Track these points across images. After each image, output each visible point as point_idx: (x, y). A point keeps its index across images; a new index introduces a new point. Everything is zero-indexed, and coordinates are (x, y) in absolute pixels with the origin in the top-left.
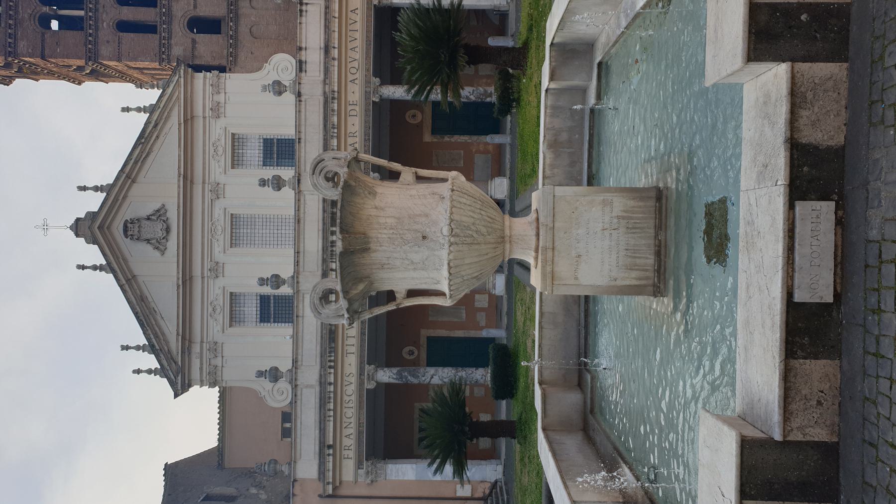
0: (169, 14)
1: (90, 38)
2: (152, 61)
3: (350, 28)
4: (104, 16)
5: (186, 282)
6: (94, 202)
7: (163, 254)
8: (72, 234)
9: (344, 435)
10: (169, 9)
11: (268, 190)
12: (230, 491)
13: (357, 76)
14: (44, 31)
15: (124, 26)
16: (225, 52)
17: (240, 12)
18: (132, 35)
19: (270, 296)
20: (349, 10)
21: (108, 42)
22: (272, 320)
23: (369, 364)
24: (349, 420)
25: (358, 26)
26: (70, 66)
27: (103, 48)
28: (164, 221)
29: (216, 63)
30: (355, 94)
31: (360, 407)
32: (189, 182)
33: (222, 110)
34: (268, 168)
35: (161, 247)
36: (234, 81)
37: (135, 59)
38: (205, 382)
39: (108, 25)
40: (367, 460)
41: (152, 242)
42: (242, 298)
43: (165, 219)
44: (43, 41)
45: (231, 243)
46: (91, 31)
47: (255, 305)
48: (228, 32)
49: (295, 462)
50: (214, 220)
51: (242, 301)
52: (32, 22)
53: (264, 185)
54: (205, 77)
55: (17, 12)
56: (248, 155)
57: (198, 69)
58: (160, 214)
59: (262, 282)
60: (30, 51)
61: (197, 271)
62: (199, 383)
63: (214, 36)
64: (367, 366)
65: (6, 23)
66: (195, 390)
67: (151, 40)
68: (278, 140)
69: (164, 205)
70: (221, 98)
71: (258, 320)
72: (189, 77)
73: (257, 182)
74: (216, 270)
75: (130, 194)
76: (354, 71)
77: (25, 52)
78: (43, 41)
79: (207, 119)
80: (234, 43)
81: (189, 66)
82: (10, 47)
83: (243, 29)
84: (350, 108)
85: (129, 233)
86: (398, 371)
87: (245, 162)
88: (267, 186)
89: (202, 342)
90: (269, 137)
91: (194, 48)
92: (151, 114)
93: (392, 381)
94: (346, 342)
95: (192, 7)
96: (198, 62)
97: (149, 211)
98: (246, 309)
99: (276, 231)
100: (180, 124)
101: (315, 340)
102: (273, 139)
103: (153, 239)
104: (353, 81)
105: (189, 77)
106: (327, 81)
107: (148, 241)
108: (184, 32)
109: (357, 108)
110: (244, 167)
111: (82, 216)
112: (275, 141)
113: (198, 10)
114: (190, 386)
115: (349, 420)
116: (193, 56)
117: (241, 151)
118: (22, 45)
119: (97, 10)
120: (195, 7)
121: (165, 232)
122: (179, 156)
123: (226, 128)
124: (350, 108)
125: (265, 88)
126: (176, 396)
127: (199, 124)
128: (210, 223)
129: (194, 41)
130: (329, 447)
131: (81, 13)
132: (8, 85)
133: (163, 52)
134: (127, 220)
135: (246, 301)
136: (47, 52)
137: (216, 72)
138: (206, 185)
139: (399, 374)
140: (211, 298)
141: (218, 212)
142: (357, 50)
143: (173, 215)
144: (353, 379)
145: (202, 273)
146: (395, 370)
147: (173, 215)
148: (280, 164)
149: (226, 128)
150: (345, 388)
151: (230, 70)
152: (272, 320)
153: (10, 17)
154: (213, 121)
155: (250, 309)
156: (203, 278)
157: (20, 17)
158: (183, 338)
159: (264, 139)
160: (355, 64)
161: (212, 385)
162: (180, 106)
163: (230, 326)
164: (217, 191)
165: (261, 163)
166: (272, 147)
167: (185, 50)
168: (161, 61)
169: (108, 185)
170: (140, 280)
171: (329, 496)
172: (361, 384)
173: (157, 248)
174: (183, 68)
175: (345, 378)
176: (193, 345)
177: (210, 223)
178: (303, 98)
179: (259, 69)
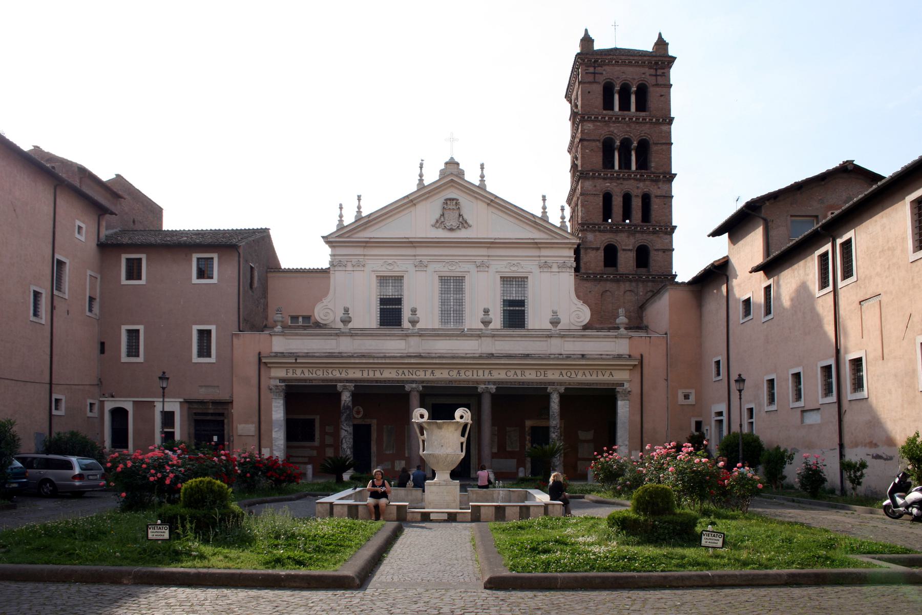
0: (617, 232)
1: (597, 174)
2: (582, 218)
3: (600, 372)
4: (615, 184)
5: (411, 244)
6: (472, 176)
7: (433, 226)
8: (447, 160)
9: (304, 369)
10: (621, 231)
11: (481, 314)
12: (256, 284)
13: (565, 377)
14: (602, 141)
15: (607, 198)
16: (591, 272)
17: (621, 283)
18: (601, 204)
19: (401, 305)
20: (612, 371)
21: (595, 186)
22: (382, 307)
23: (355, 386)
24: (314, 373)
25: (600, 377)
26: (577, 159)
27: (591, 183)
28: (458, 227)
29: (582, 265)
30: (553, 376)
31: (323, 380)
32: (489, 245)
33: (545, 270)
34: (502, 303)
35: (438, 225)
36: (568, 279)
37: (582, 206)
38: (333, 258)
39: (608, 187)
40: (286, 386)
41: (442, 218)
42: (399, 284)
43: (460, 227)
44: (594, 140)
45: (442, 277)
46: (602, 175)
47: (394, 294)
48: (605, 274)
49: (283, 335)
50: (460, 264)
51: (396, 285)
52: (607, 133)
53: (485, 312)
54: (570, 257)
55: (614, 122)
56: (511, 289)
57: (577, 252)
58: (464, 224)
59: (414, 311)
60: (586, 131)
61: (420, 251)
62: (334, 253)
63: (602, 264)
64: (353, 384)
65: (606, 115)
66: (327, 250)
67: (598, 218)
68: (524, 310)
69: (471, 226)
70: (555, 269)
71: (382, 297)
72: (570, 246)
73: (486, 307)
74: (421, 266)
75: (480, 203)
76: (569, 374)
77: (584, 127)
78: (594, 140)
79: (538, 259)
80: (596, 278)
81: (579, 245)
82: (588, 117)
83: (609, 286)
84: (542, 372)
85: (449, 202)
86: (350, 406)
87: (505, 286)
88: (484, 313)
89: (364, 255)
90: (526, 304)
91: (593, 249)
92: (540, 218)
93: (343, 403)
94: (370, 370)
95: (624, 248)
96: (582, 251)
97: (465, 217)
98: (391, 287)
99: (452, 309)
100: (533, 239)
101: (371, 348)
102: (524, 306)
103: (445, 219)
104: (561, 374)
105: (570, 246)
106: (561, 356)
107: (443, 215)
108: (605, 241)
109: (542, 377)
110: (502, 285)
111: (461, 167)
112: (523, 308)
113: (622, 252)
114: (330, 247)
115: (314, 373)
116: (586, 249)
117: (514, 283)
118: (589, 126)
119: (618, 179)
120: (624, 250)
121: (450, 227)
122: (510, 239)
123: (531, 272)
124: (542, 372)
125: (555, 313)
126: (323, 237)
127: (535, 252)
128: (457, 261)
129: (597, 249)
130: (296, 360)
131: (617, 167)
132: (566, 97)
133: (588, 227)
134: (458, 200)
135: (397, 288)
136: (585, 143)
137: (574, 265)
138: (487, 258)
139: (348, 407)
140: (399, 262)
141: (465, 267)
142: (584, 377)
143: (462, 234)
144: (344, 375)
145: (418, 255)
146: (350, 404)
147: (462, 234)
148: (505, 312)
149: (531, 272)
150: (337, 370)
151: (577, 275)
152: (382, 307)
153: (610, 118)
154: (536, 263)
155: (390, 290)
156: (415, 256)
157: (611, 125)
158: (367, 242)
159: (524, 300)
160: (573, 375)
161: (332, 263)
162: (547, 239)
163: (377, 276)
164: (482, 266)
165: (505, 298)
166: (518, 306)
167: (591, 242)
168: (582, 225)
169: (485, 186)
170: (412, 209)
171: (260, 360)
172: (341, 381)
173: (437, 221)
174: (578, 241)
175: (344, 370)
176: (362, 249)
177: (457, 261)
178: (549, 339)
179: (578, 297)
